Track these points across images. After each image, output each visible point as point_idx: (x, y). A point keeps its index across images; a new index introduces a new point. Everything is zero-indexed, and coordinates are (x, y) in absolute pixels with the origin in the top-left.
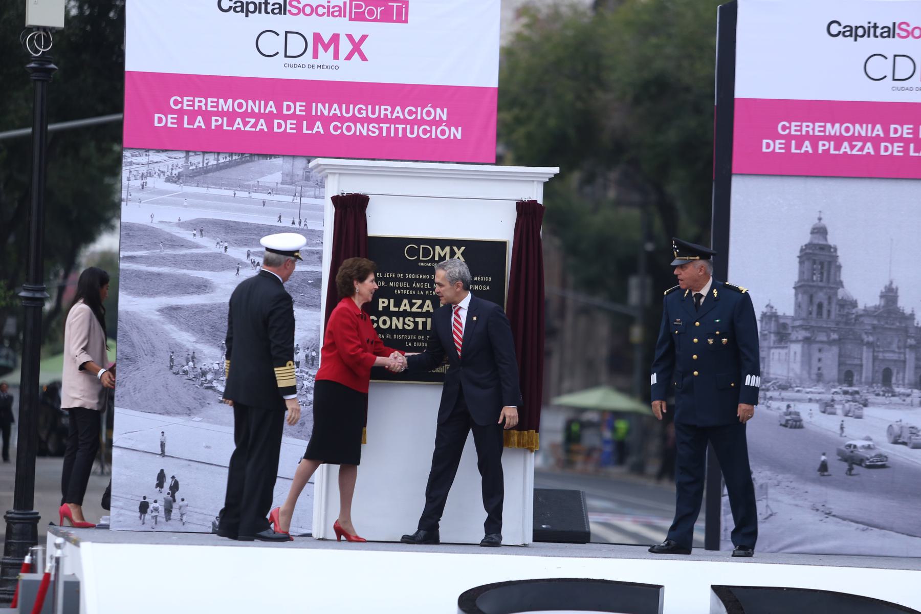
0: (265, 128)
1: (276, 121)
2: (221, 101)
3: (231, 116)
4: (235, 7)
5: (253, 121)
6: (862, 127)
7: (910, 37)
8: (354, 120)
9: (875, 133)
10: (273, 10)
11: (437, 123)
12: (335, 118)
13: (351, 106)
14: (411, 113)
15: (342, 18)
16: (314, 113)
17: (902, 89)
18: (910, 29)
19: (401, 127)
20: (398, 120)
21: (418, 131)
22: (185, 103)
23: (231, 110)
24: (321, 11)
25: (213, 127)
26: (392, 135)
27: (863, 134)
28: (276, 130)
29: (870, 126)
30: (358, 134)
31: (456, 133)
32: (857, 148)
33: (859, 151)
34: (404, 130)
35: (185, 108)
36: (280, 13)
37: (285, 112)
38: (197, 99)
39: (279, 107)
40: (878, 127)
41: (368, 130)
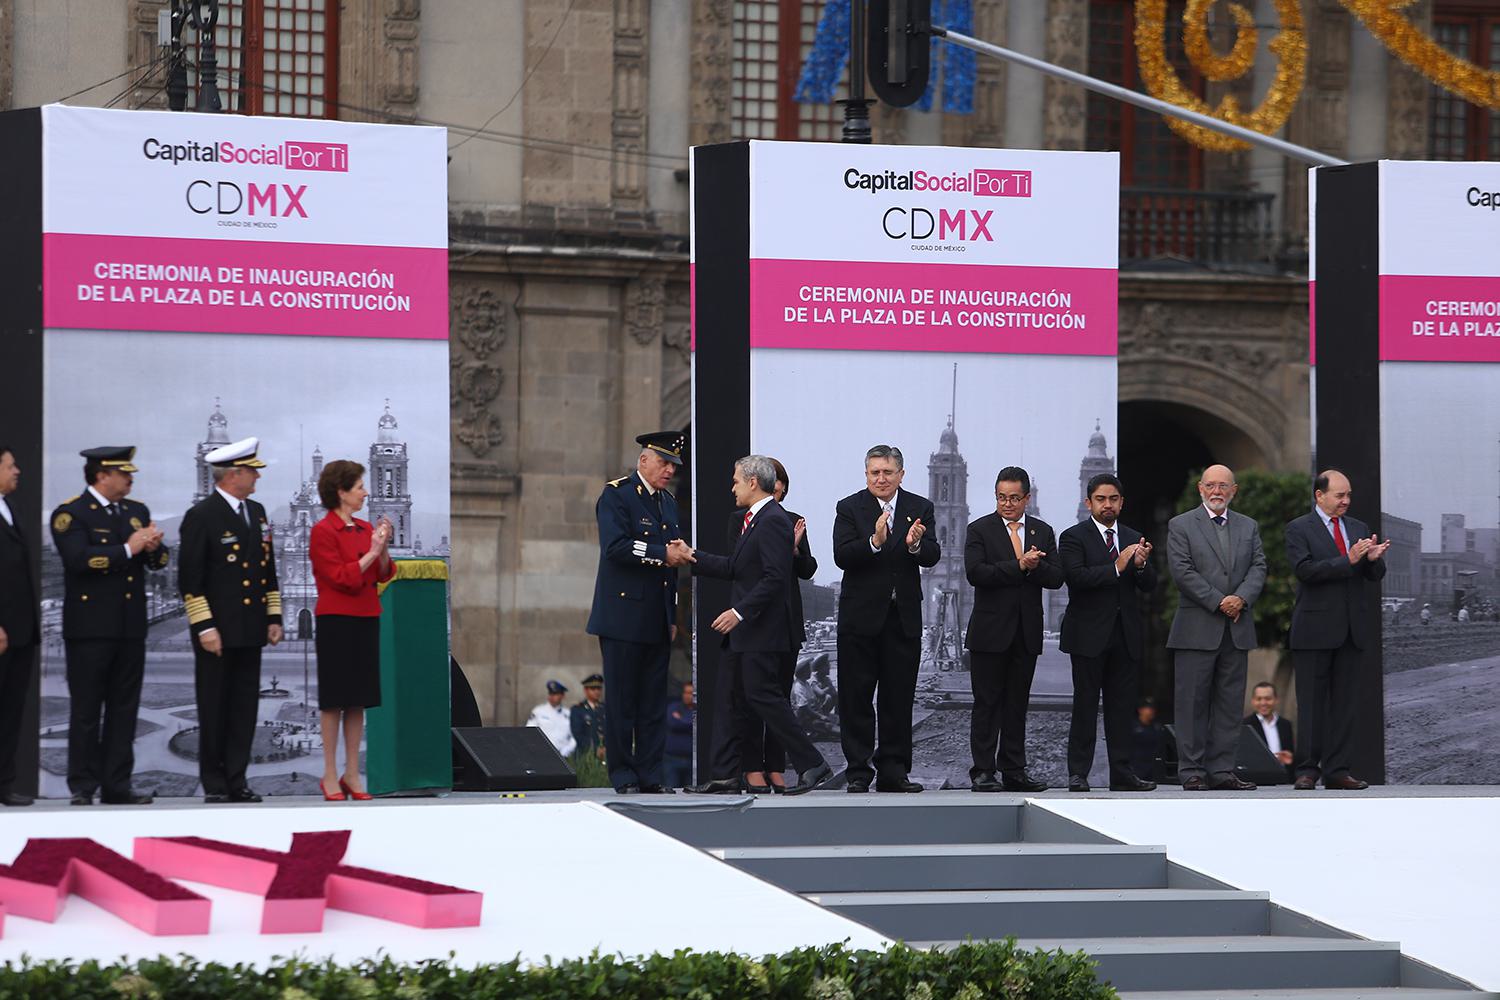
0: (894, 320)
1: (905, 312)
2: (850, 290)
3: (861, 307)
4: (863, 182)
5: (882, 312)
6: (187, 269)
7: (235, 162)
8: (295, 288)
9: (203, 277)
10: (899, 184)
11: (1060, 310)
12: (275, 287)
13: (978, 293)
14: (355, 279)
15: (968, 192)
16: (942, 302)
17: (229, 224)
18: (233, 151)
19: (345, 296)
20: (342, 289)
21: (364, 302)
22: (815, 294)
23: (860, 300)
24: (947, 184)
25: (843, 321)
26: (337, 306)
27: (190, 279)
28: (905, 322)
29: (196, 268)
30: (300, 305)
31: (404, 303)
32: (184, 296)
33: (185, 299)
34: (1030, 318)
35: (815, 299)
36: (906, 188)
37: (913, 301)
38: (826, 289)
39: (907, 296)
40: (206, 270)
41: (995, 320)
